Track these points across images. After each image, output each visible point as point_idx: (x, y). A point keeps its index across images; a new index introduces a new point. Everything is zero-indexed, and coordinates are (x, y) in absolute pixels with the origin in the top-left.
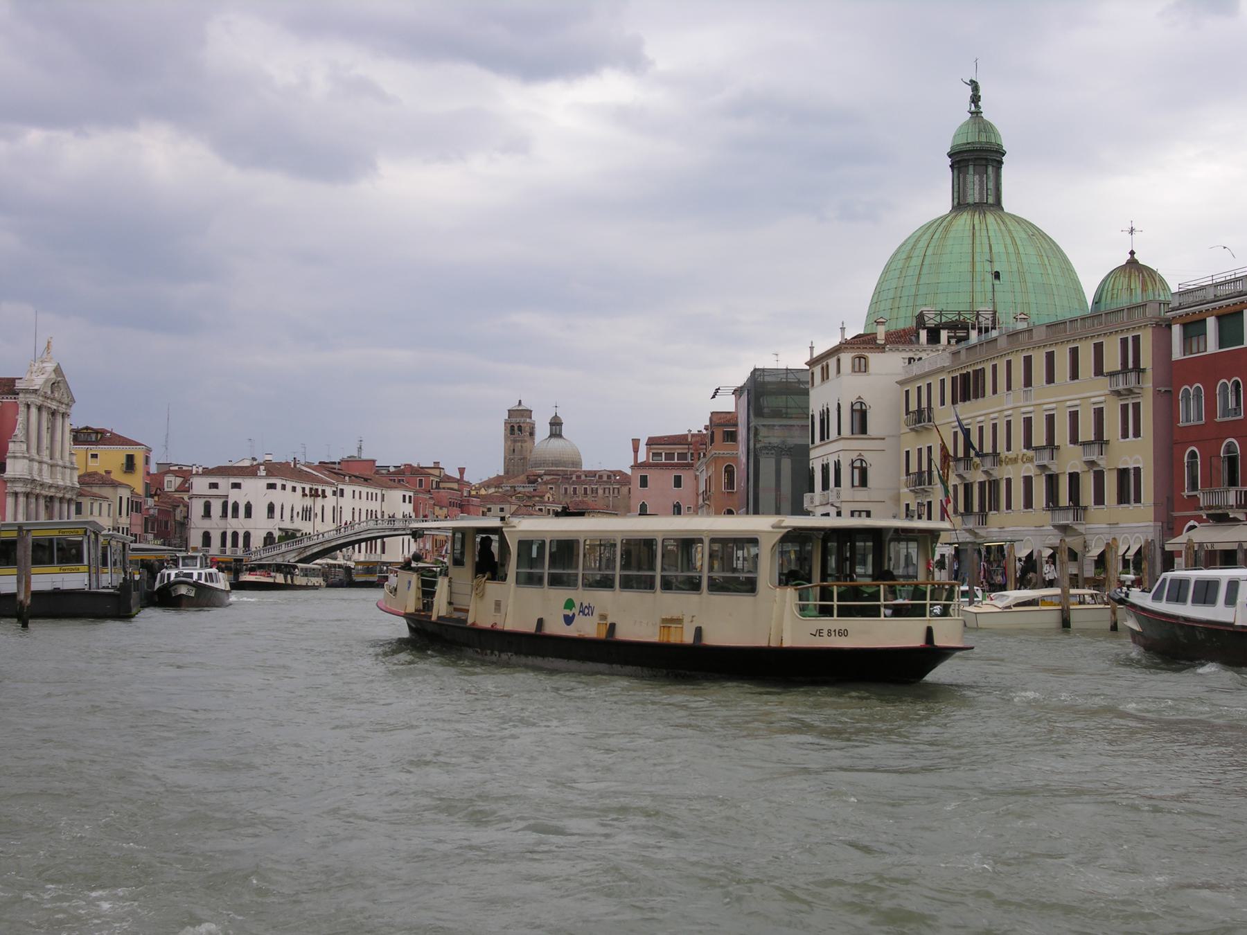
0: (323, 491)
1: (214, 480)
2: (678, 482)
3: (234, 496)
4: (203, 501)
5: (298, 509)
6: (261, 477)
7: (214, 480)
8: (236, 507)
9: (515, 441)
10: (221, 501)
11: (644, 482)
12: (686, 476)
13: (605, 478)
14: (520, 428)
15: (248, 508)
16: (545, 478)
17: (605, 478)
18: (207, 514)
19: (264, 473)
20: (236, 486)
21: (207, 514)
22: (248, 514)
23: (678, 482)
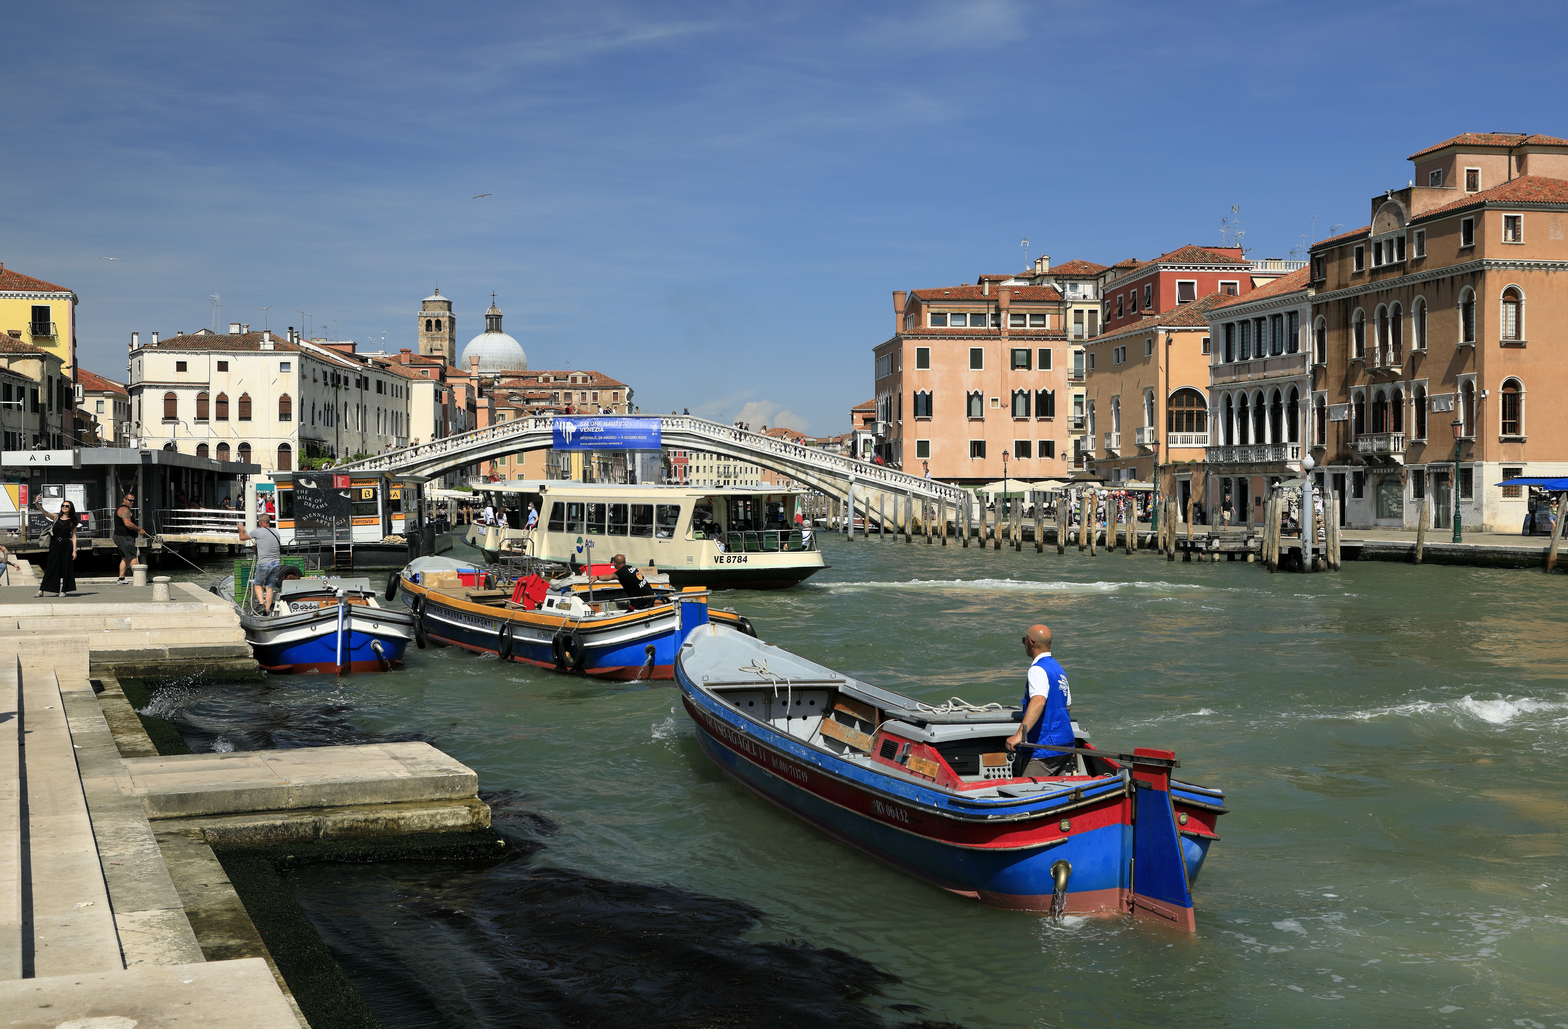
0: (346, 379)
1: (182, 358)
2: (976, 359)
3: (219, 384)
4: (162, 393)
5: (320, 407)
6: (266, 354)
7: (182, 358)
8: (222, 401)
9: (433, 339)
10: (194, 393)
11: (923, 359)
12: (986, 347)
13: (579, 381)
14: (438, 323)
15: (245, 403)
16: (503, 381)
17: (579, 381)
18: (170, 416)
19: (270, 346)
20: (223, 366)
21: (170, 416)
22: (245, 415)
23: (976, 359)
